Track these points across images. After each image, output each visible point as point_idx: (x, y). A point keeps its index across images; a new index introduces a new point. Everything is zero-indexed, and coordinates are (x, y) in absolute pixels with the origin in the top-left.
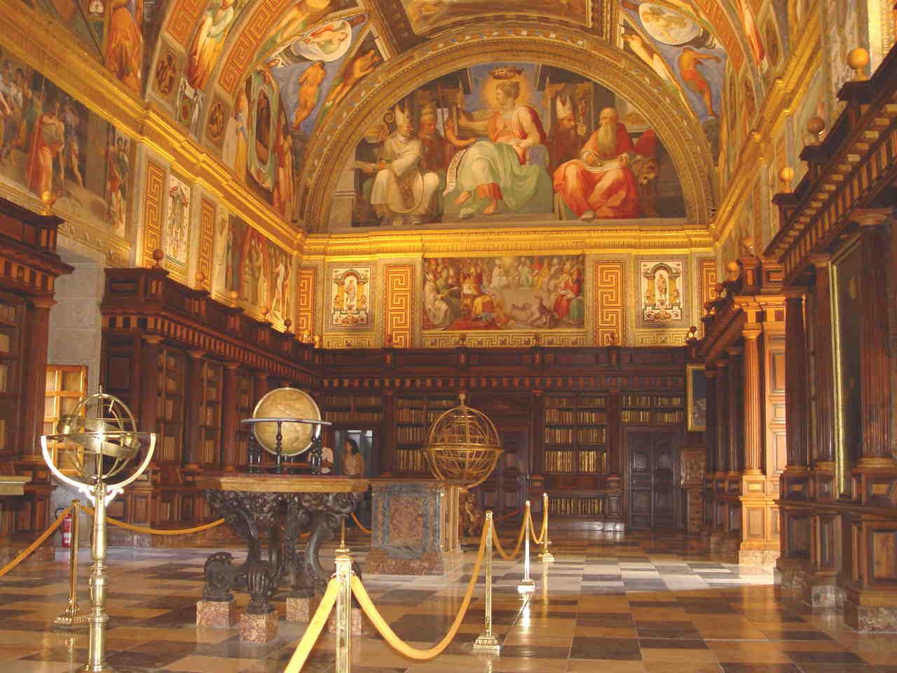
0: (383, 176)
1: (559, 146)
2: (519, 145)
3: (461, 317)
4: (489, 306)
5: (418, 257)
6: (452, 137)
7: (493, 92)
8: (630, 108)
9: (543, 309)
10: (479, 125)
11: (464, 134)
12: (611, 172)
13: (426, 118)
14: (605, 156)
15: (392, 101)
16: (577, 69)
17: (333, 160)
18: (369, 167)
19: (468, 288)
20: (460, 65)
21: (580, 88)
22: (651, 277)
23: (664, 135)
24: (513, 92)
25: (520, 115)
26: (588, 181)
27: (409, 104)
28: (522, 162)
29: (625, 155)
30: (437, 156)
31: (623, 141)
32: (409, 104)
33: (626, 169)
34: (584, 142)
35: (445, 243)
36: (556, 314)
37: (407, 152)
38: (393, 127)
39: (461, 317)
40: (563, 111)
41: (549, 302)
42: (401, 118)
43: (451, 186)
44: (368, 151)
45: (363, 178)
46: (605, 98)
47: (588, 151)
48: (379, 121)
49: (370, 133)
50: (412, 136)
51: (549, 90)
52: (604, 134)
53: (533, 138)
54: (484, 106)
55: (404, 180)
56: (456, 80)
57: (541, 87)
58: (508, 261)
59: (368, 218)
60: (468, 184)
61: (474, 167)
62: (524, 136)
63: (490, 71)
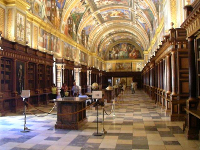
0: (112, 54)
1: (129, 51)
2: (125, 51)
3: (120, 68)
4: (123, 68)
5: (116, 63)
6: (119, 50)
7: (123, 46)
8: (136, 48)
9: (128, 68)
10: (121, 49)
11: (120, 50)
12: (134, 54)
13: (116, 48)
14: (134, 52)
15: (112, 47)
16: (131, 44)
17: (107, 53)
18: (110, 54)
19: (121, 66)
20: (119, 43)
21: (131, 46)
22: (138, 64)
23: (140, 50)
24: (125, 46)
25: (125, 48)
26: (132, 55)
27: (114, 47)
28: (126, 53)
29: (136, 52)
30: (117, 52)
31: (135, 51)
32: (114, 47)
33: (136, 54)
34: (132, 51)
35: (118, 61)
36: (129, 68)
37: (114, 52)
38: (113, 50)
39: (120, 68)
40: (130, 48)
41: (129, 67)
42: (114, 48)
43: (119, 55)
44: (110, 52)
45: (110, 55)
46: (134, 46)
47: (132, 52)
48: (111, 49)
49: (110, 50)
50: (115, 50)
51: (128, 46)
52: (134, 50)
53: (127, 51)
54: (121, 47)
55: (114, 55)
56: (119, 45)
57: (127, 45)
58: (124, 63)
59: (111, 59)
60: (120, 55)
61: (121, 54)
62: (126, 50)
63: (122, 44)
